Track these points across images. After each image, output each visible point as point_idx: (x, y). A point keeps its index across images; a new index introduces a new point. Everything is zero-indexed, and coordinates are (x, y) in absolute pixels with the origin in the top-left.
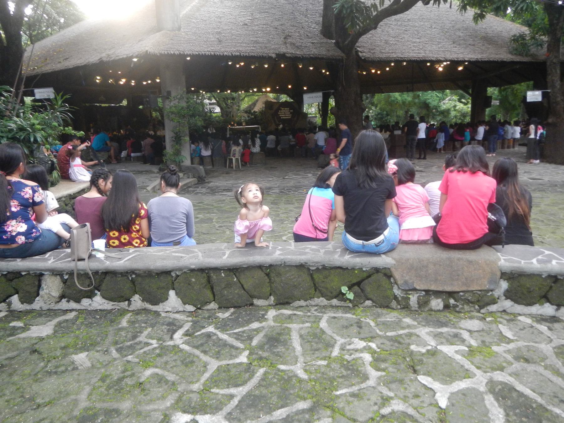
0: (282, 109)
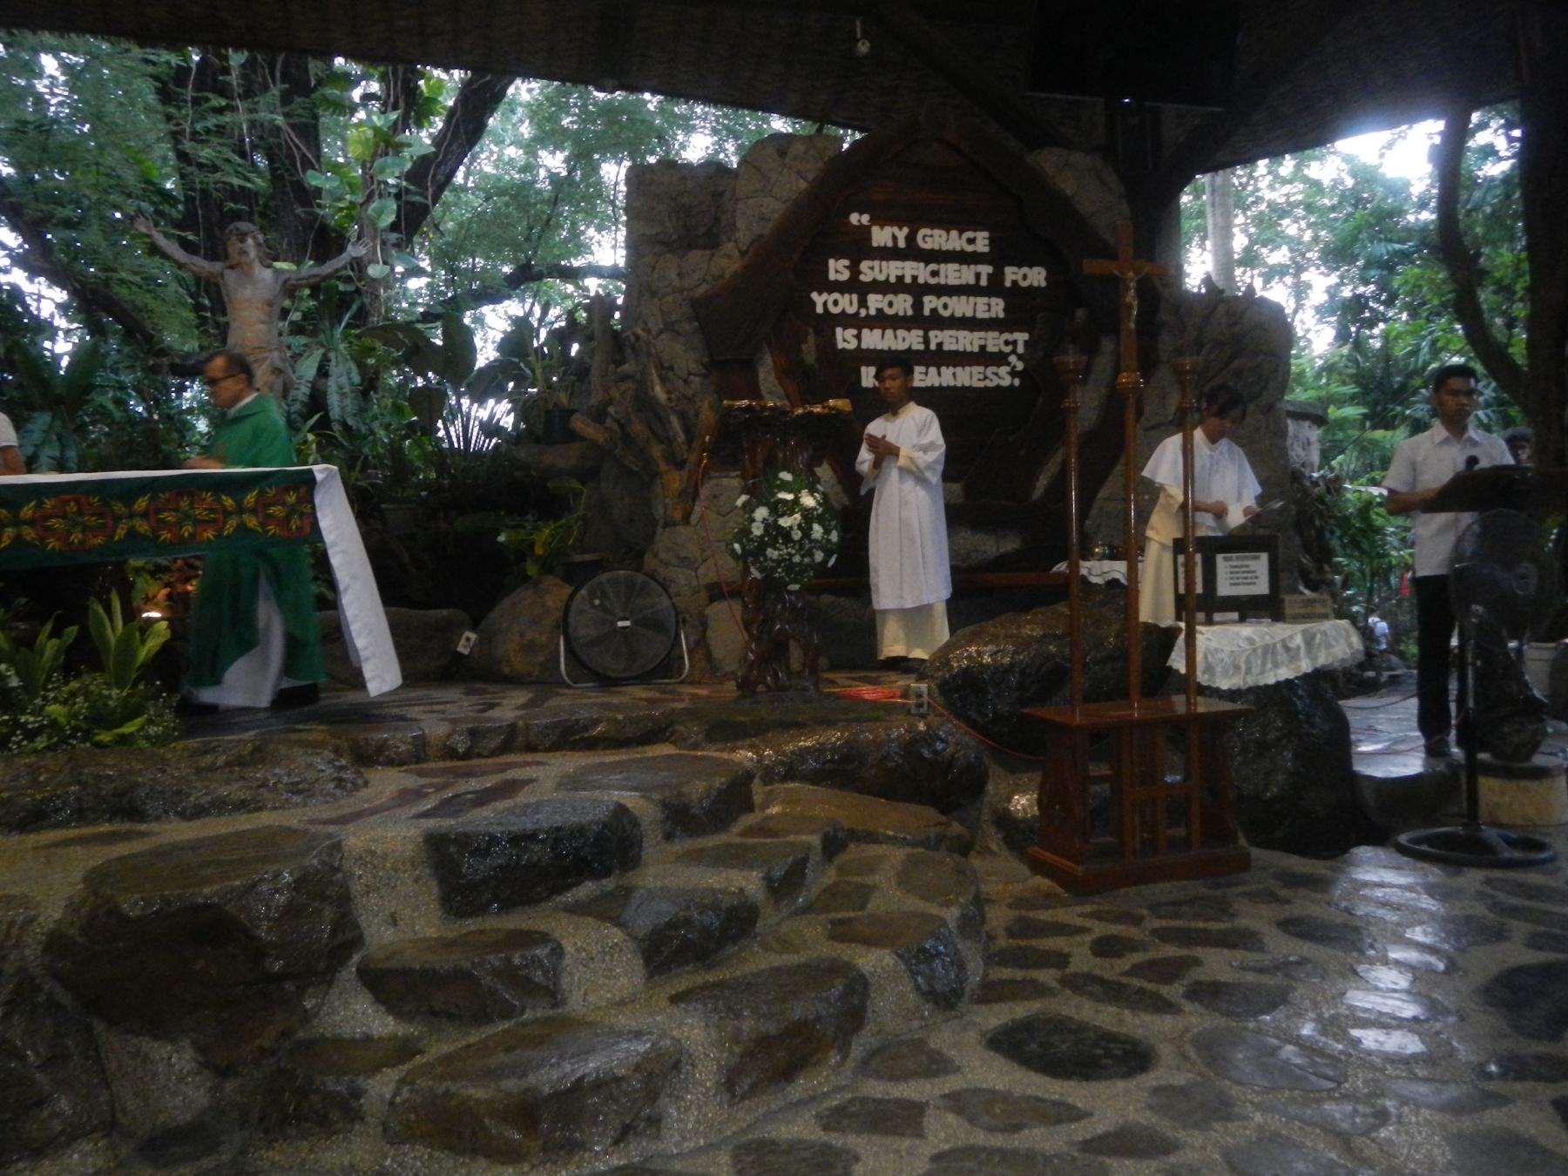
0: (881, 236)
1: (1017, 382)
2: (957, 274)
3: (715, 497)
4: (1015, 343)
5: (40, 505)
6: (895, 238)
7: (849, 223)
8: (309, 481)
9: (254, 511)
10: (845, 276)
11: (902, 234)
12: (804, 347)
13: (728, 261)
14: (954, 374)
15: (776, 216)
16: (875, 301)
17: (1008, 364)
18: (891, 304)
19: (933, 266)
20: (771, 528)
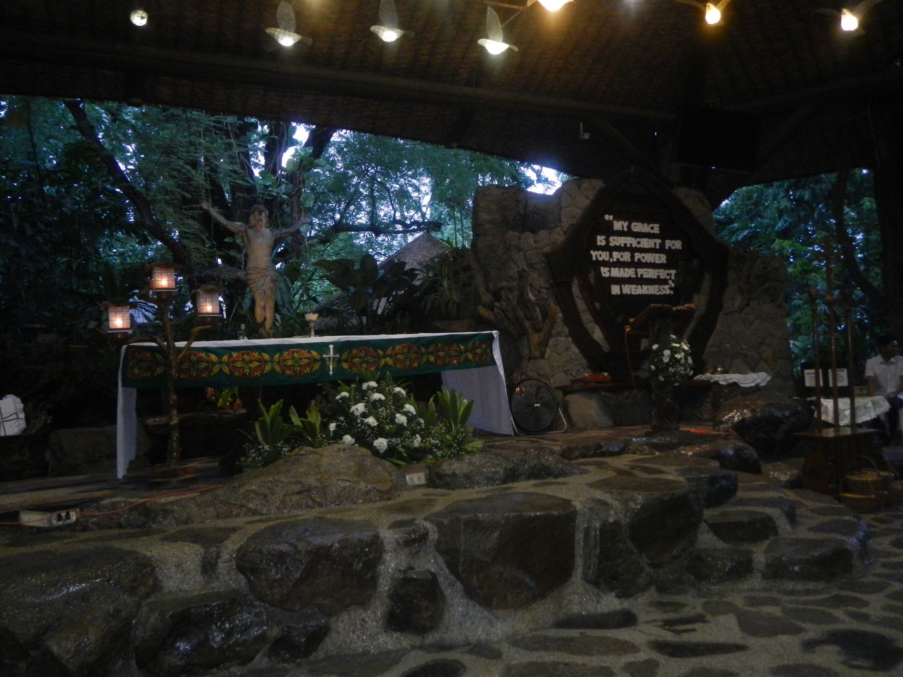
0: (618, 225)
1: (672, 292)
2: (648, 243)
3: (556, 345)
4: (670, 275)
5: (394, 348)
6: (623, 226)
7: (605, 219)
8: (491, 338)
9: (470, 351)
10: (604, 243)
11: (626, 224)
12: (590, 276)
14: (648, 289)
15: (578, 216)
16: (616, 255)
17: (668, 284)
18: (622, 256)
19: (638, 240)
20: (672, 357)
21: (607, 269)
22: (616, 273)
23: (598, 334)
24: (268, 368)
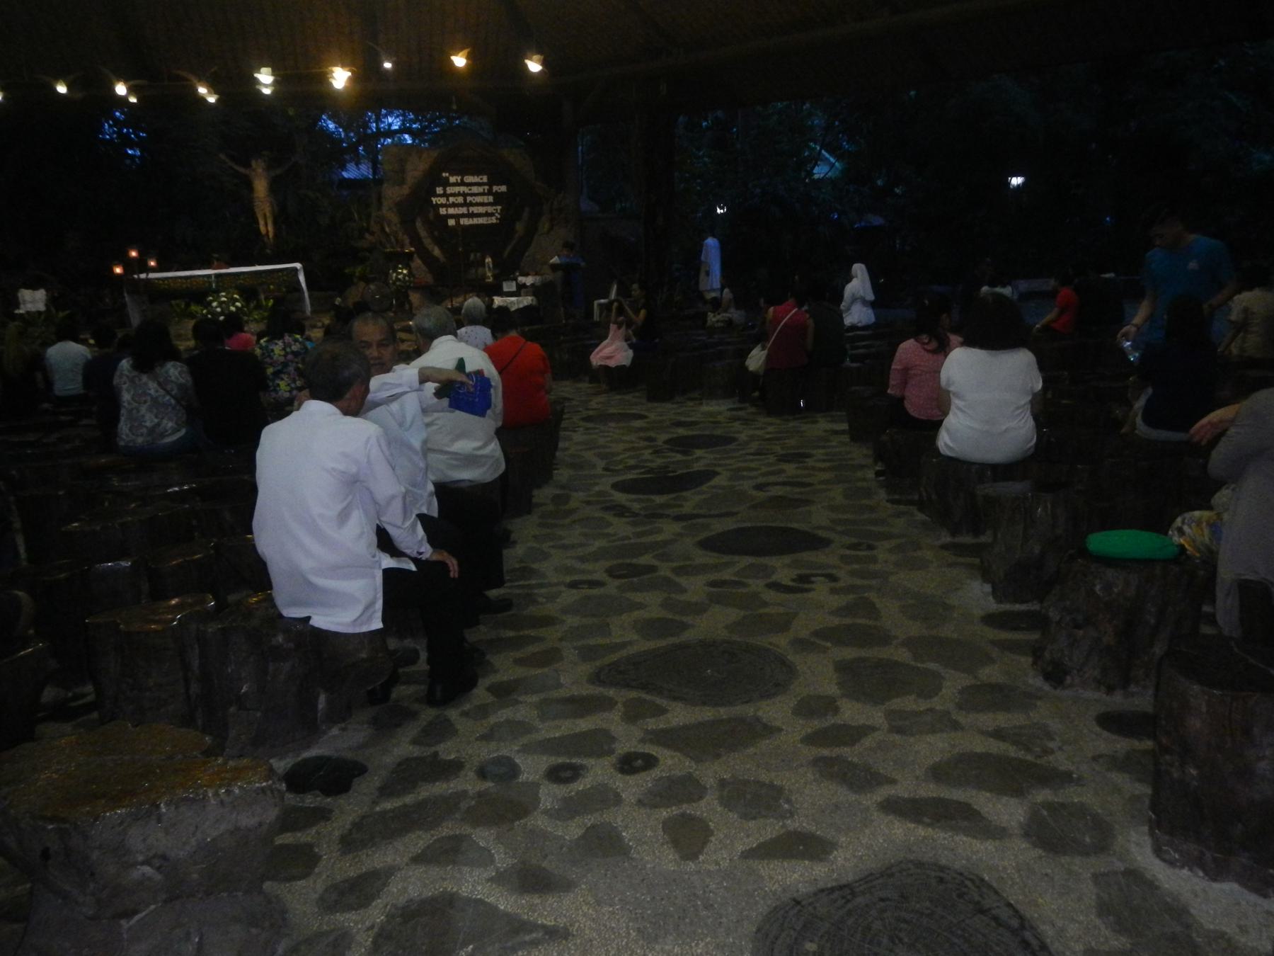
0: (452, 179)
6: (457, 180)
10: (442, 192)
11: (459, 178)
13: (405, 190)
16: (451, 199)
18: (456, 200)
19: (470, 188)
20: (397, 278)
21: (444, 209)
22: (451, 211)
23: (437, 252)
24: (184, 286)
